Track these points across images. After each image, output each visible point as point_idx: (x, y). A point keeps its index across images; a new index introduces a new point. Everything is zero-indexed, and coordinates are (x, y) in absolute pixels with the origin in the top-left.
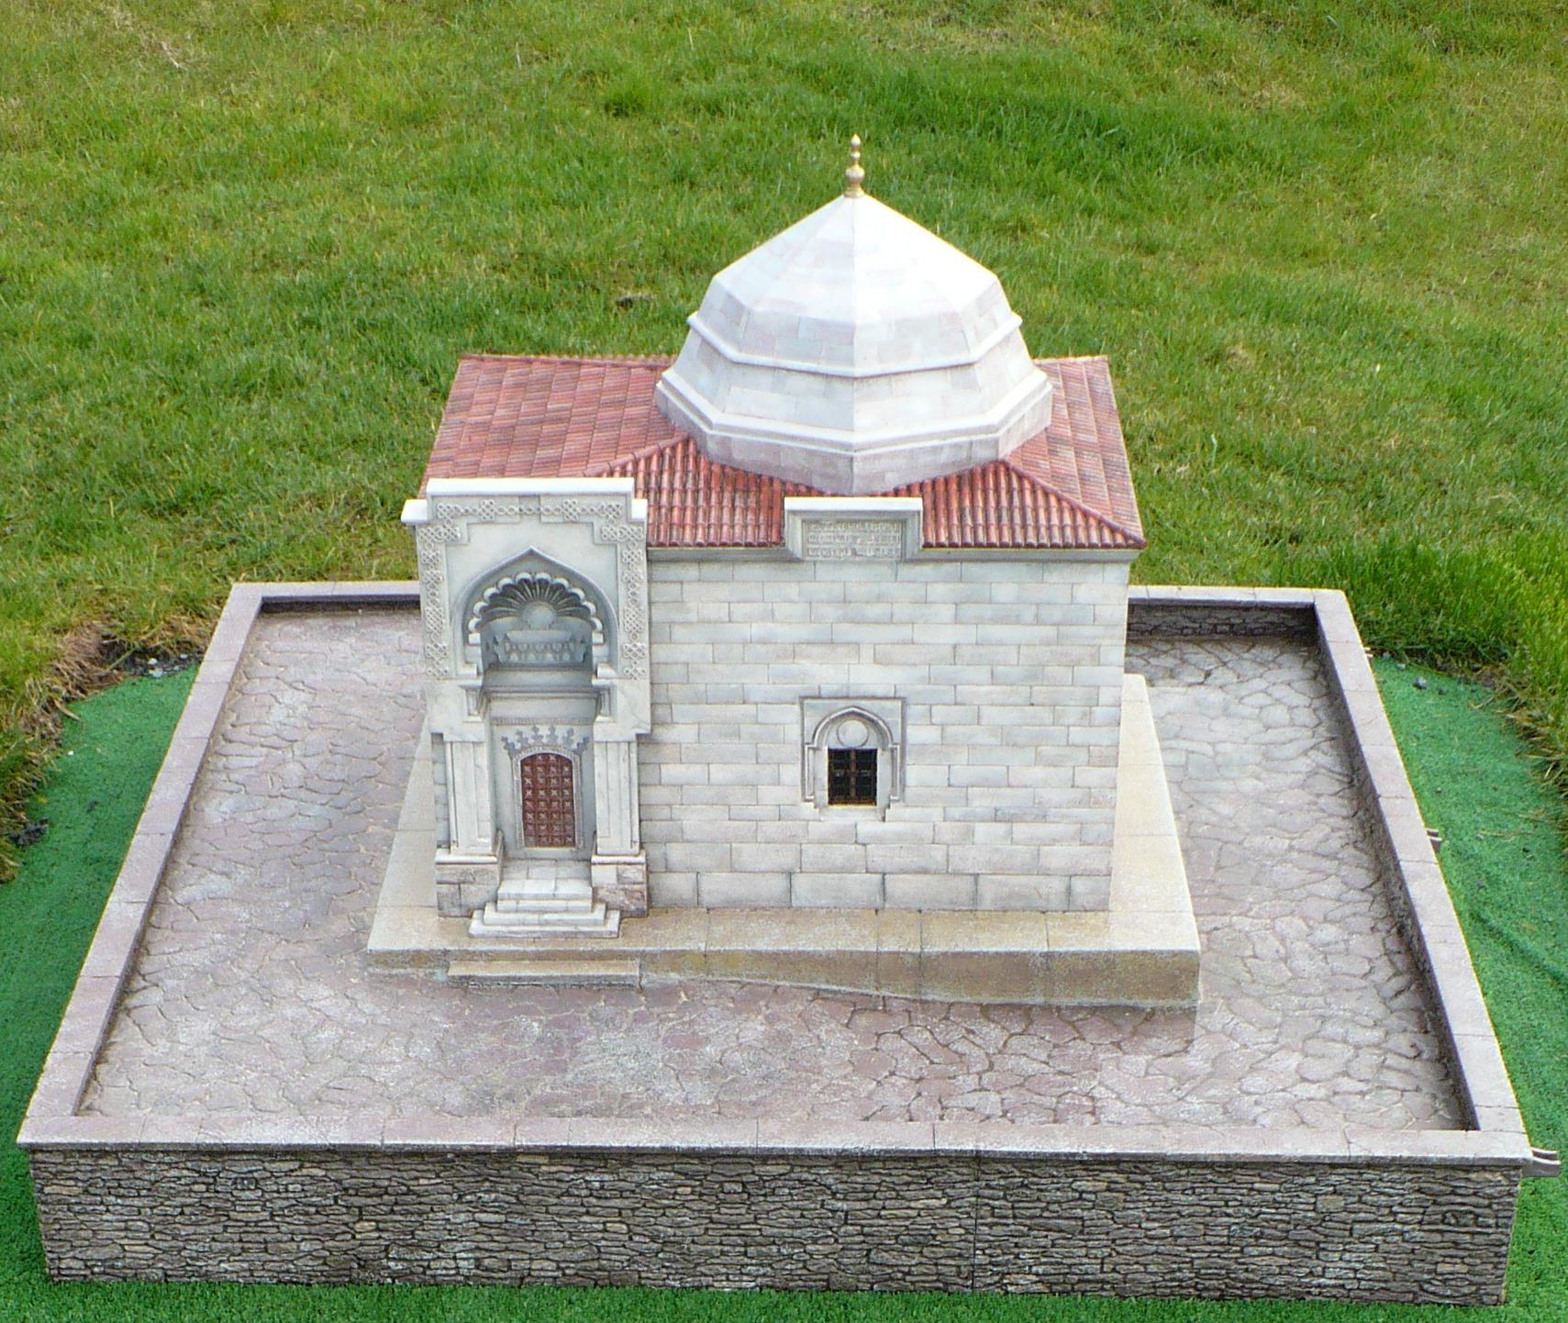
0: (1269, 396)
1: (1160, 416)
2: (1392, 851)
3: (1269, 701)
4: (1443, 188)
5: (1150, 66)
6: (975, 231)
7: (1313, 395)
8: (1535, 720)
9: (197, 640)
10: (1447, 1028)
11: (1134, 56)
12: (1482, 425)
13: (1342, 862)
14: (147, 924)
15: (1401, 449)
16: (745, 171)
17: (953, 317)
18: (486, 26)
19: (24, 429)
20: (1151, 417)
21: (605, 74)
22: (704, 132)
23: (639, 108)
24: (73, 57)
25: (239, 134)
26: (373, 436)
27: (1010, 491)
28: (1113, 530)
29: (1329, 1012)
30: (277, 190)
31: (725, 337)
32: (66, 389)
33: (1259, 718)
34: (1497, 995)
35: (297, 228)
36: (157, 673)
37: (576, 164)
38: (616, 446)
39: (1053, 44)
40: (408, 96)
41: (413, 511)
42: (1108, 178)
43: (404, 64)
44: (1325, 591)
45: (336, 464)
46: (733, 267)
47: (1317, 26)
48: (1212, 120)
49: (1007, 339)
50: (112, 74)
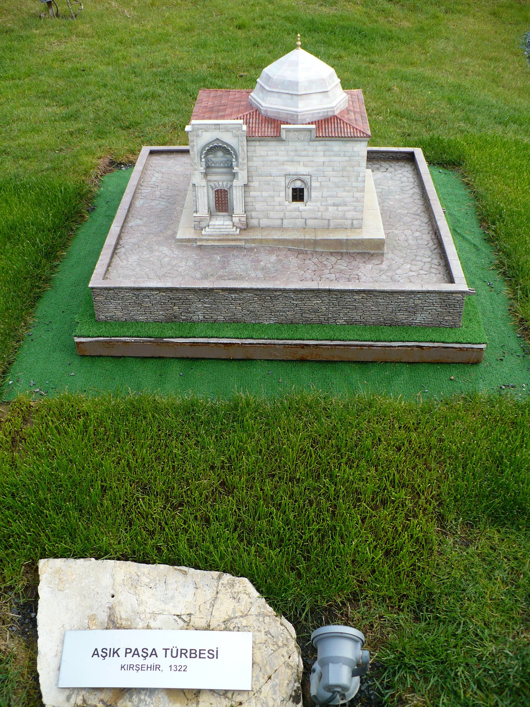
0: (402, 99)
1: (375, 104)
2: (433, 214)
3: (402, 176)
4: (446, 47)
5: (372, 17)
6: (329, 58)
7: (413, 99)
8: (469, 181)
9: (134, 161)
10: (447, 258)
11: (369, 14)
12: (456, 107)
13: (421, 216)
14: (121, 232)
15: (435, 112)
16: (271, 43)
17: (323, 80)
18: (206, 6)
19: (90, 108)
20: (373, 105)
21: (236, 18)
22: (261, 33)
23: (244, 27)
24: (102, 14)
25: (144, 34)
26: (178, 109)
27: (337, 123)
28: (363, 133)
29: (417, 254)
30: (153, 48)
31: (266, 85)
32: (101, 98)
33: (400, 180)
34: (460, 250)
35: (158, 57)
36: (124, 169)
37: (229, 41)
38: (239, 112)
39: (348, 11)
40: (187, 24)
41: (188, 128)
42: (362, 45)
43: (186, 16)
44: (416, 148)
45: (168, 116)
46: (268, 67)
47: (414, 6)
48: (388, 30)
49: (337, 85)
50: (112, 18)
